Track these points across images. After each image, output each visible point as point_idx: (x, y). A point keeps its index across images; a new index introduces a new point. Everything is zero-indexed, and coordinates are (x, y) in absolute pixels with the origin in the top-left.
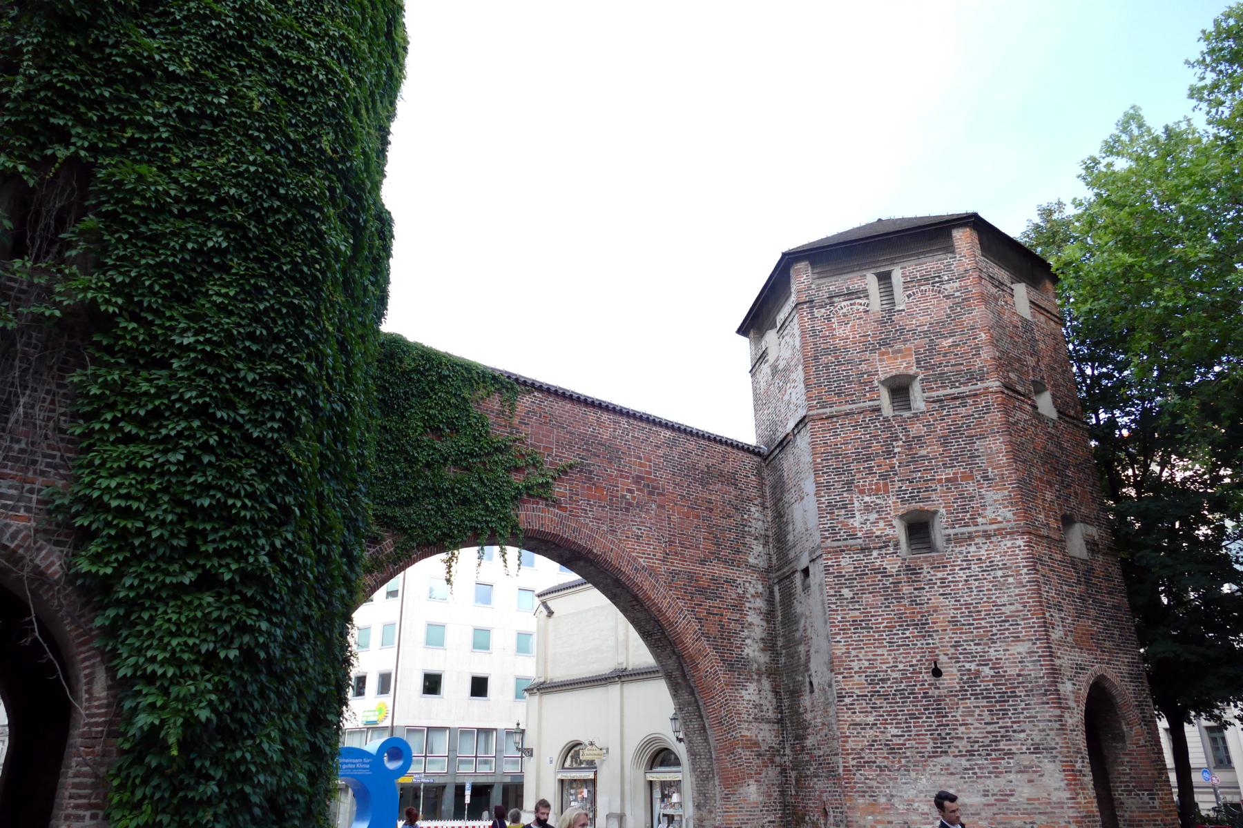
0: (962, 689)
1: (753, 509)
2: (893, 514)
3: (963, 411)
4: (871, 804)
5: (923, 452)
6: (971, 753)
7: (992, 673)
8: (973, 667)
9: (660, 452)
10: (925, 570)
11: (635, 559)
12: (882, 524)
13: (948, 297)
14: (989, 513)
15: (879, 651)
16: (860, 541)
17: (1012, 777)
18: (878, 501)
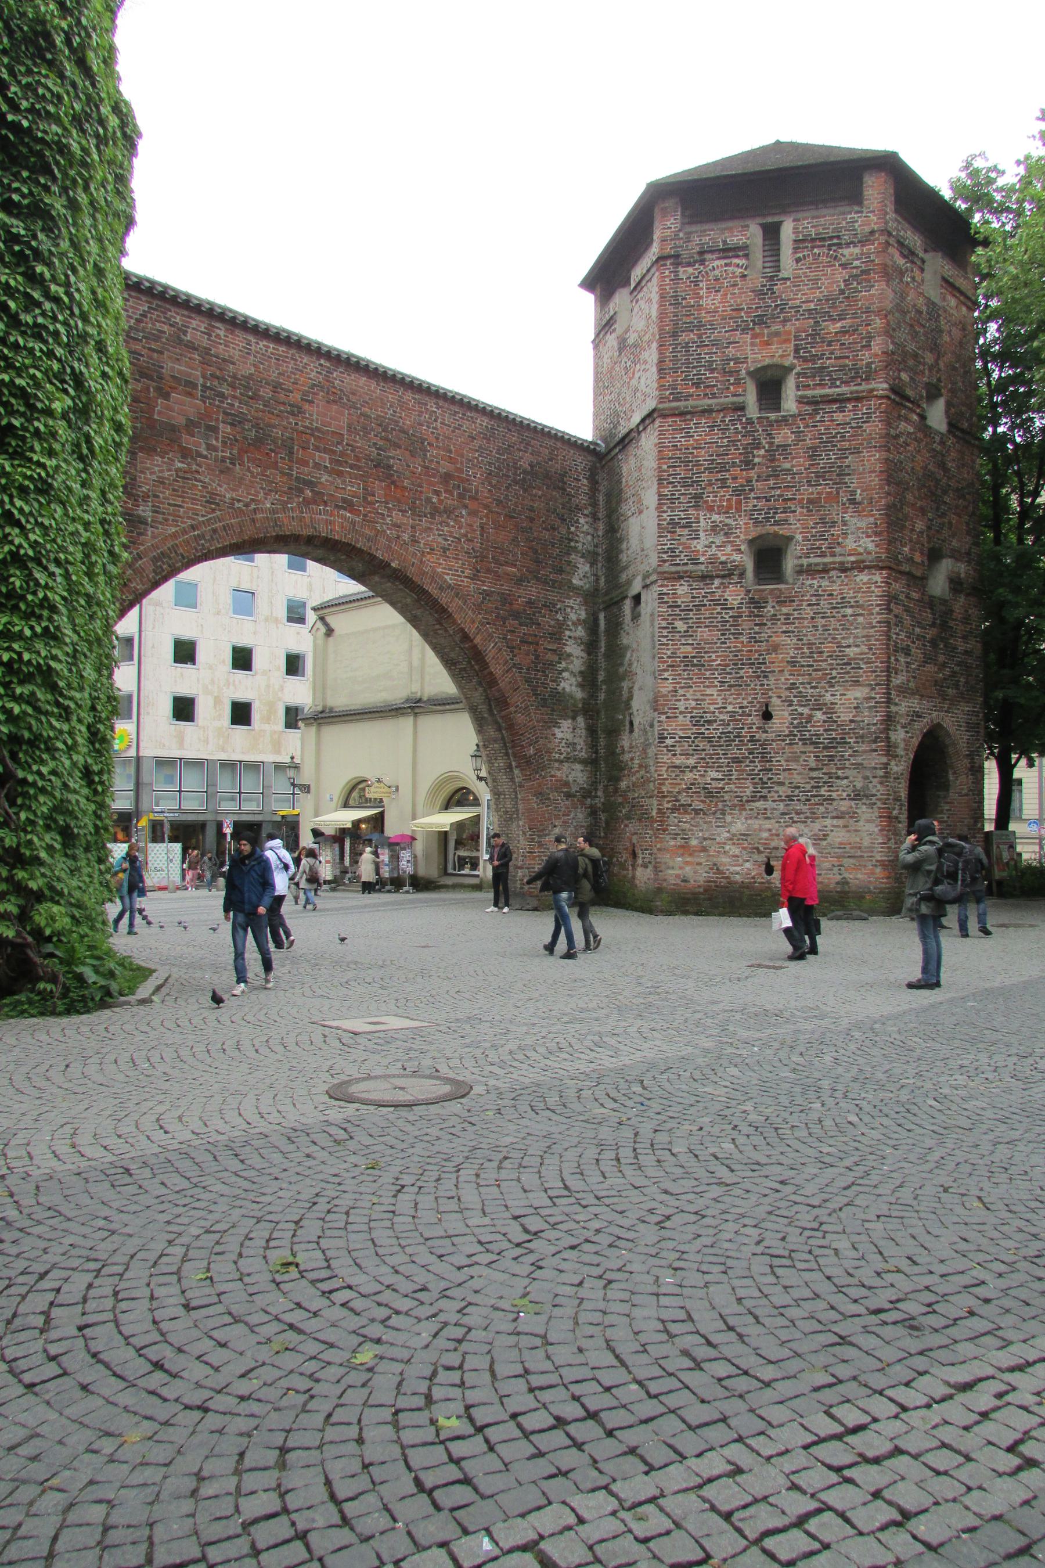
0: (791, 734)
1: (582, 520)
2: (742, 537)
3: (839, 417)
4: (682, 847)
5: (787, 466)
6: (790, 798)
7: (824, 717)
8: (806, 711)
9: (476, 443)
10: (771, 604)
12: (729, 549)
13: (844, 266)
14: (850, 543)
15: (709, 691)
16: (702, 567)
17: (828, 822)
18: (727, 521)
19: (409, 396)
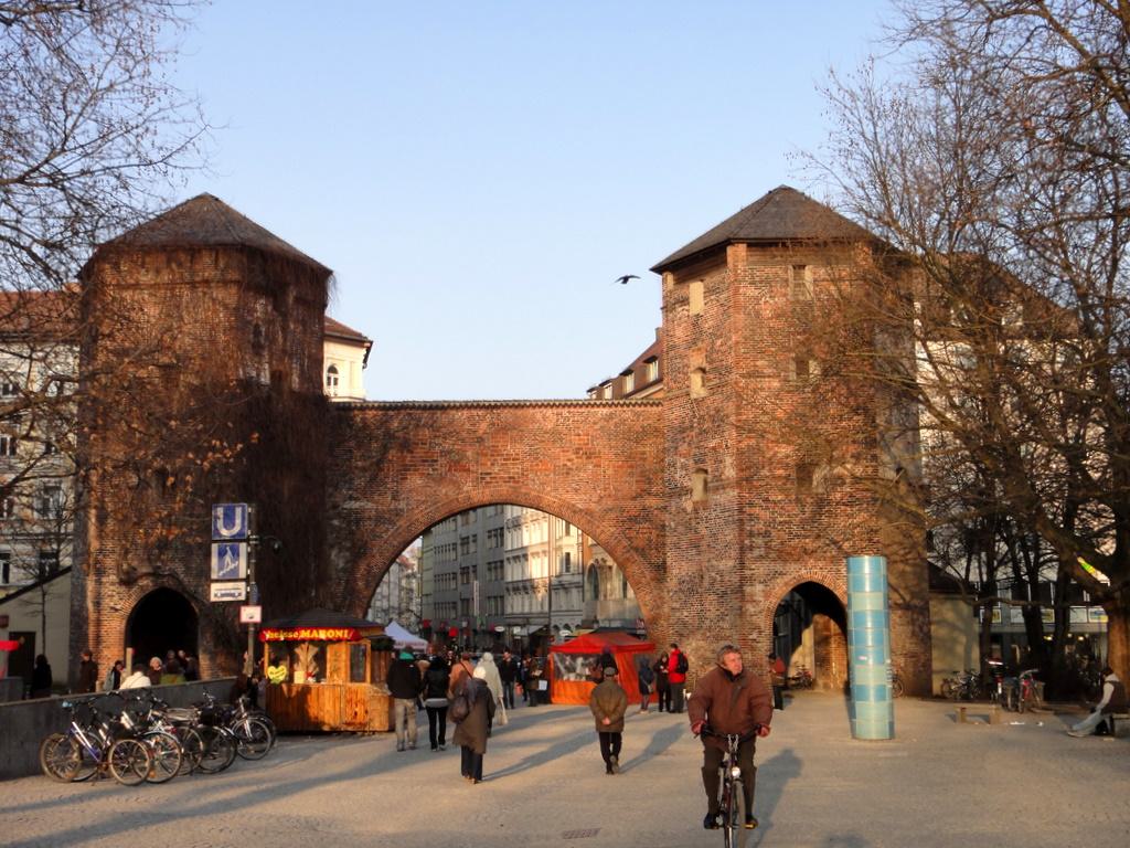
8: (713, 574)
9: (597, 427)
11: (573, 505)
12: (687, 478)
19: (549, 412)
